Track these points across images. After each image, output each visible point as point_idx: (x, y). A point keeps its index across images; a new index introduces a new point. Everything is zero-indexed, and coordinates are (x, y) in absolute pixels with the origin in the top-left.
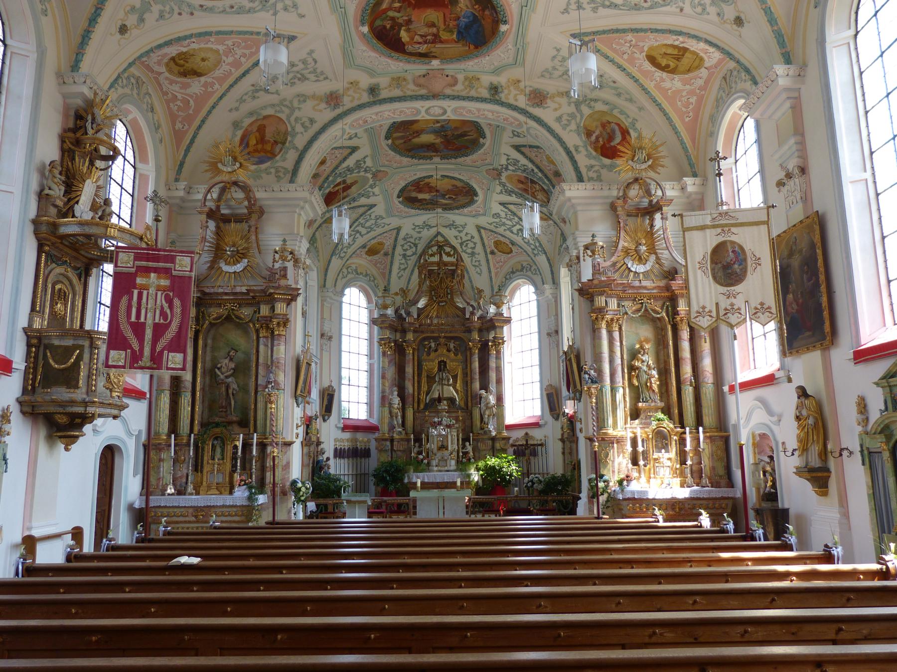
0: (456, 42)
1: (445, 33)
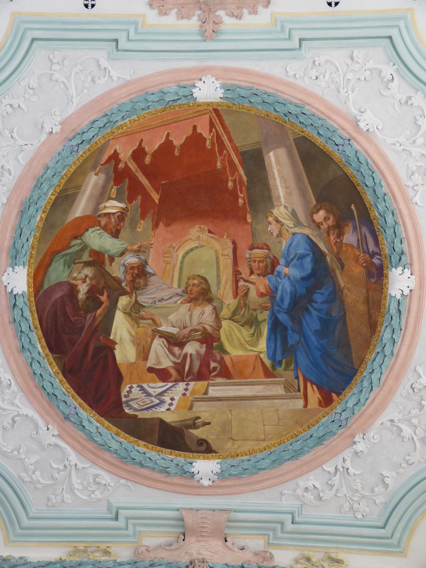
0: (268, 374)
1: (233, 325)
